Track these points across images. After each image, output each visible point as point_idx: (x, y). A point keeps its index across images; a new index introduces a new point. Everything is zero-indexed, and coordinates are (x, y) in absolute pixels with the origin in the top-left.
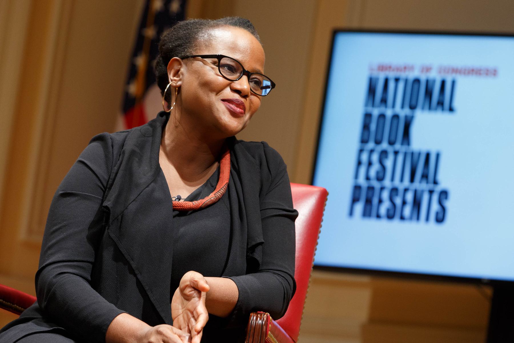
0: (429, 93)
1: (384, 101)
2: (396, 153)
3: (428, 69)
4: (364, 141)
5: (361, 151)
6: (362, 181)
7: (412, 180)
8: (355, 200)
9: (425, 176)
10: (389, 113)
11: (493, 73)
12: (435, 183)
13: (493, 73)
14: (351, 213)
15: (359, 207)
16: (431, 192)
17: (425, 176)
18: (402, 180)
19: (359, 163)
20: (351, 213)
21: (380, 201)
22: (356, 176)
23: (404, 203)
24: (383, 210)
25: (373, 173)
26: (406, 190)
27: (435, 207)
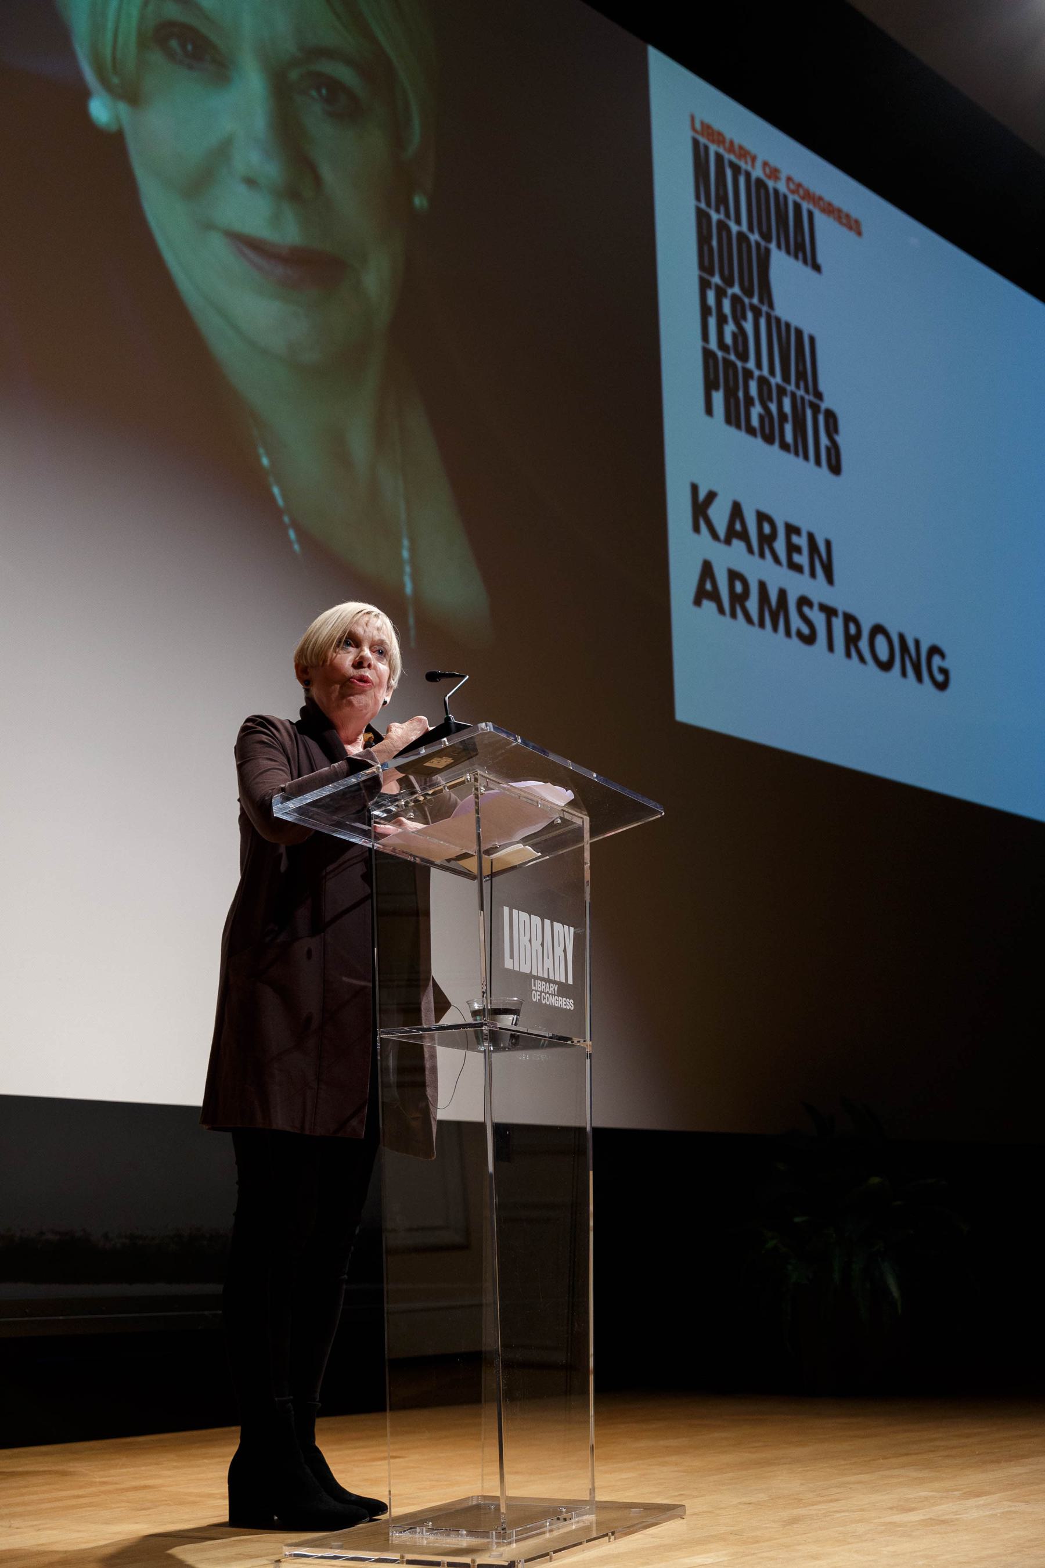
0: (782, 218)
1: (722, 200)
2: (757, 313)
3: (775, 174)
4: (705, 267)
5: (704, 285)
6: (713, 345)
7: (786, 378)
8: (710, 386)
9: (801, 375)
10: (734, 228)
11: (854, 226)
12: (819, 395)
13: (854, 226)
14: (709, 411)
15: (718, 397)
16: (816, 409)
17: (801, 375)
18: (772, 372)
19: (705, 311)
20: (709, 411)
21: (749, 402)
22: (705, 337)
23: (783, 417)
24: (755, 422)
25: (728, 340)
26: (782, 392)
27: (824, 441)
